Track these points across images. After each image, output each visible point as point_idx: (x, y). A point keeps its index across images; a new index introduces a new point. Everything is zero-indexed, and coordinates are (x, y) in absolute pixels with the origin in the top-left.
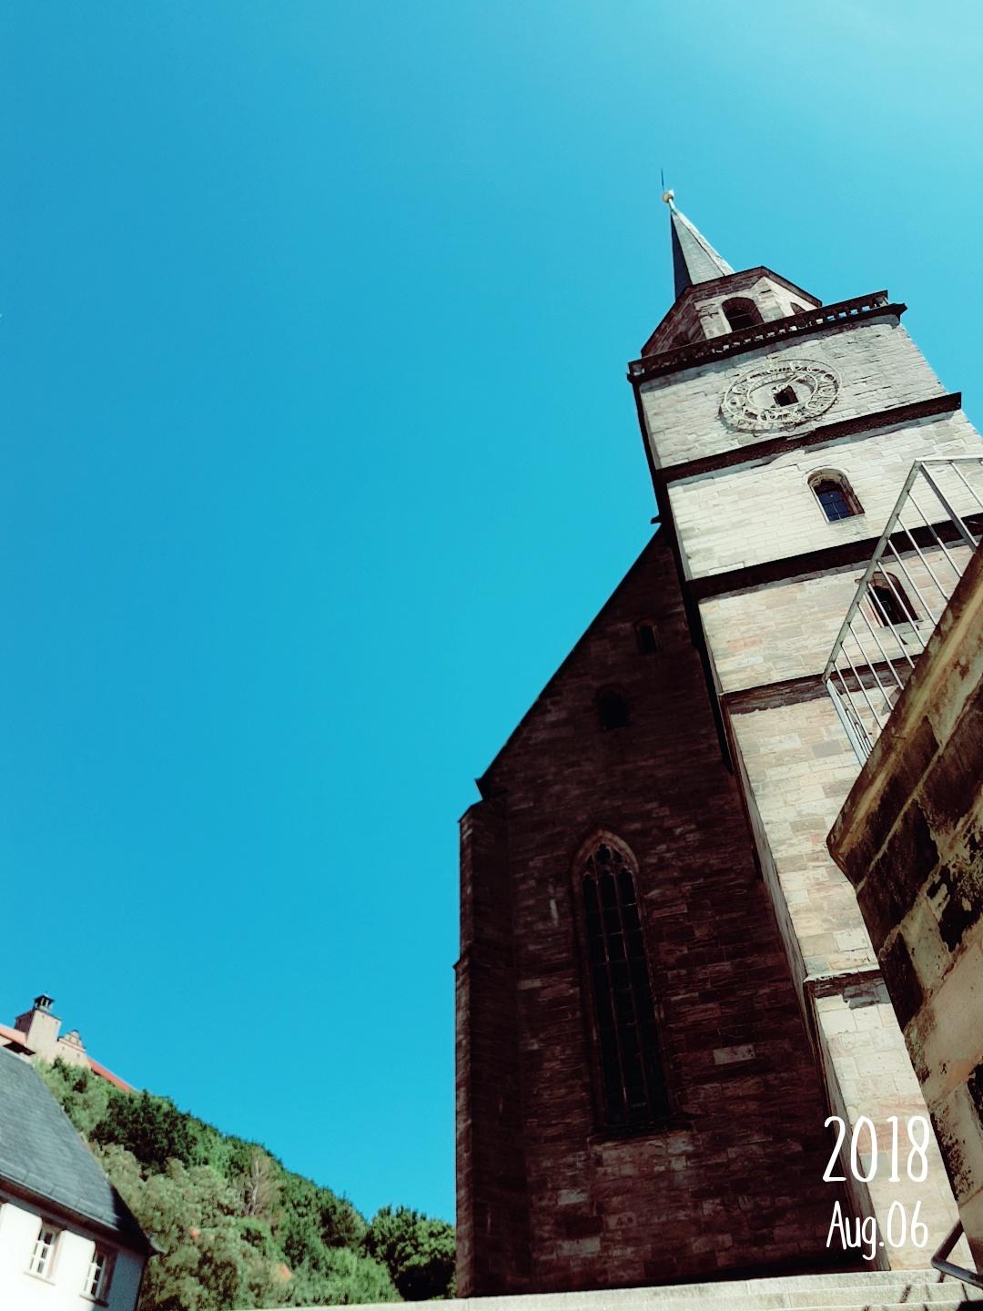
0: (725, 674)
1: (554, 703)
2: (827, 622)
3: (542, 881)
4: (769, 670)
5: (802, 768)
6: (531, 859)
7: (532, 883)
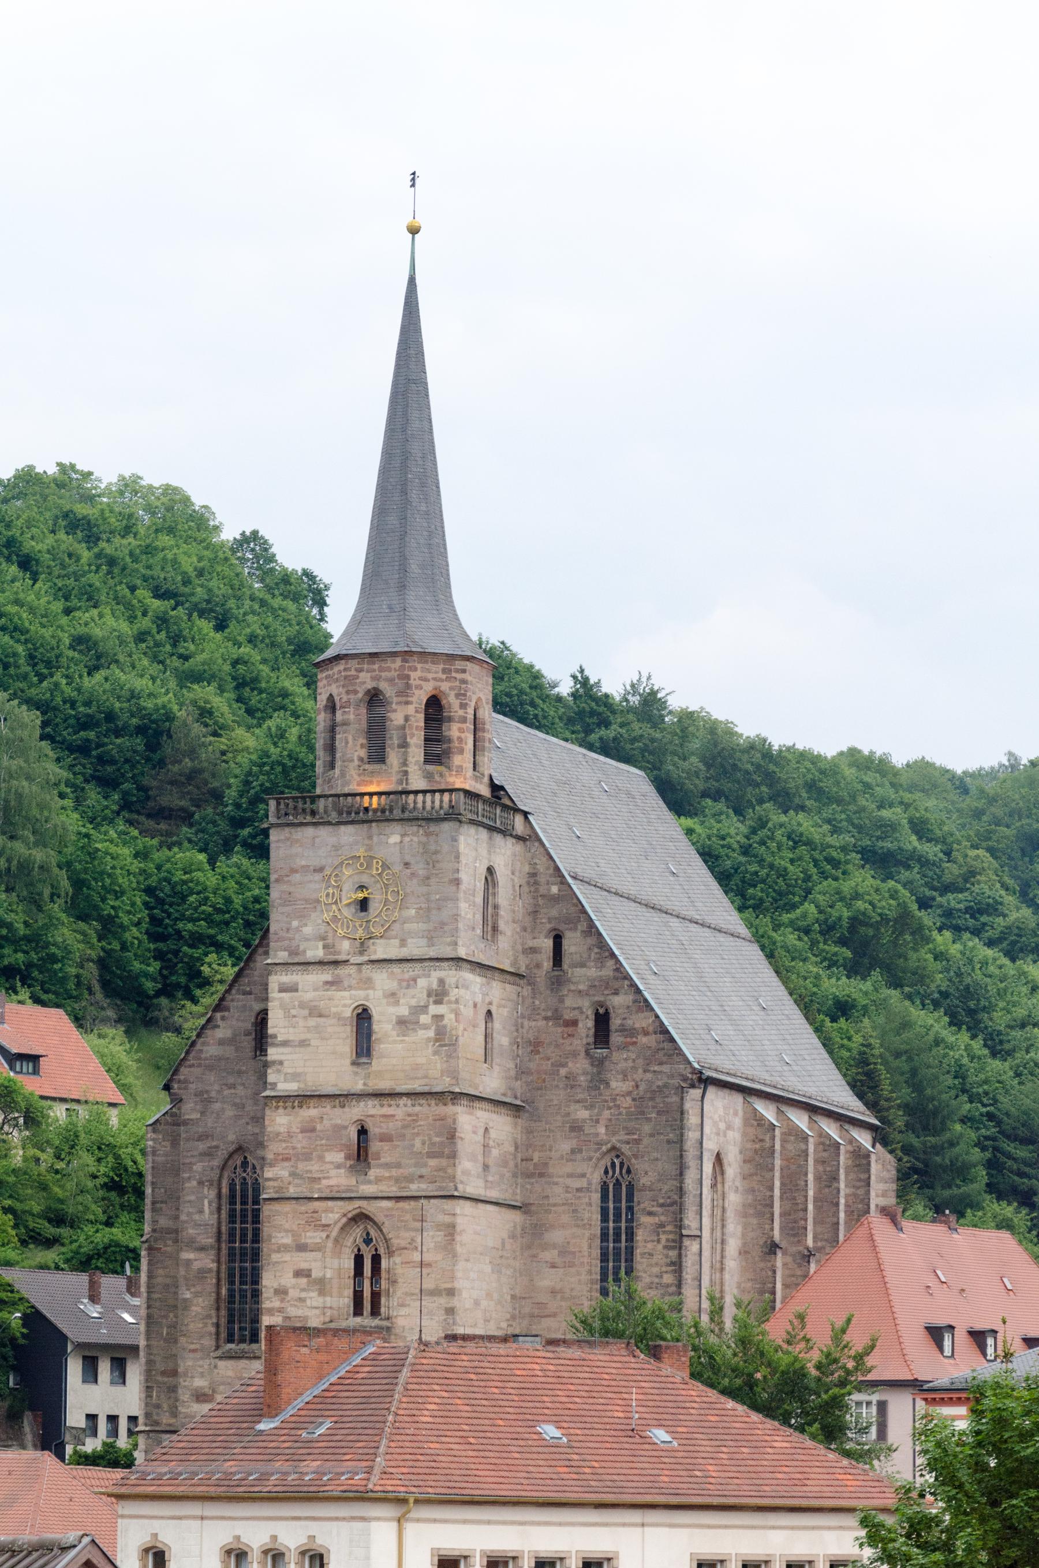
1: (223, 1018)
2: (327, 1154)
3: (201, 1183)
5: (287, 1257)
7: (194, 1183)
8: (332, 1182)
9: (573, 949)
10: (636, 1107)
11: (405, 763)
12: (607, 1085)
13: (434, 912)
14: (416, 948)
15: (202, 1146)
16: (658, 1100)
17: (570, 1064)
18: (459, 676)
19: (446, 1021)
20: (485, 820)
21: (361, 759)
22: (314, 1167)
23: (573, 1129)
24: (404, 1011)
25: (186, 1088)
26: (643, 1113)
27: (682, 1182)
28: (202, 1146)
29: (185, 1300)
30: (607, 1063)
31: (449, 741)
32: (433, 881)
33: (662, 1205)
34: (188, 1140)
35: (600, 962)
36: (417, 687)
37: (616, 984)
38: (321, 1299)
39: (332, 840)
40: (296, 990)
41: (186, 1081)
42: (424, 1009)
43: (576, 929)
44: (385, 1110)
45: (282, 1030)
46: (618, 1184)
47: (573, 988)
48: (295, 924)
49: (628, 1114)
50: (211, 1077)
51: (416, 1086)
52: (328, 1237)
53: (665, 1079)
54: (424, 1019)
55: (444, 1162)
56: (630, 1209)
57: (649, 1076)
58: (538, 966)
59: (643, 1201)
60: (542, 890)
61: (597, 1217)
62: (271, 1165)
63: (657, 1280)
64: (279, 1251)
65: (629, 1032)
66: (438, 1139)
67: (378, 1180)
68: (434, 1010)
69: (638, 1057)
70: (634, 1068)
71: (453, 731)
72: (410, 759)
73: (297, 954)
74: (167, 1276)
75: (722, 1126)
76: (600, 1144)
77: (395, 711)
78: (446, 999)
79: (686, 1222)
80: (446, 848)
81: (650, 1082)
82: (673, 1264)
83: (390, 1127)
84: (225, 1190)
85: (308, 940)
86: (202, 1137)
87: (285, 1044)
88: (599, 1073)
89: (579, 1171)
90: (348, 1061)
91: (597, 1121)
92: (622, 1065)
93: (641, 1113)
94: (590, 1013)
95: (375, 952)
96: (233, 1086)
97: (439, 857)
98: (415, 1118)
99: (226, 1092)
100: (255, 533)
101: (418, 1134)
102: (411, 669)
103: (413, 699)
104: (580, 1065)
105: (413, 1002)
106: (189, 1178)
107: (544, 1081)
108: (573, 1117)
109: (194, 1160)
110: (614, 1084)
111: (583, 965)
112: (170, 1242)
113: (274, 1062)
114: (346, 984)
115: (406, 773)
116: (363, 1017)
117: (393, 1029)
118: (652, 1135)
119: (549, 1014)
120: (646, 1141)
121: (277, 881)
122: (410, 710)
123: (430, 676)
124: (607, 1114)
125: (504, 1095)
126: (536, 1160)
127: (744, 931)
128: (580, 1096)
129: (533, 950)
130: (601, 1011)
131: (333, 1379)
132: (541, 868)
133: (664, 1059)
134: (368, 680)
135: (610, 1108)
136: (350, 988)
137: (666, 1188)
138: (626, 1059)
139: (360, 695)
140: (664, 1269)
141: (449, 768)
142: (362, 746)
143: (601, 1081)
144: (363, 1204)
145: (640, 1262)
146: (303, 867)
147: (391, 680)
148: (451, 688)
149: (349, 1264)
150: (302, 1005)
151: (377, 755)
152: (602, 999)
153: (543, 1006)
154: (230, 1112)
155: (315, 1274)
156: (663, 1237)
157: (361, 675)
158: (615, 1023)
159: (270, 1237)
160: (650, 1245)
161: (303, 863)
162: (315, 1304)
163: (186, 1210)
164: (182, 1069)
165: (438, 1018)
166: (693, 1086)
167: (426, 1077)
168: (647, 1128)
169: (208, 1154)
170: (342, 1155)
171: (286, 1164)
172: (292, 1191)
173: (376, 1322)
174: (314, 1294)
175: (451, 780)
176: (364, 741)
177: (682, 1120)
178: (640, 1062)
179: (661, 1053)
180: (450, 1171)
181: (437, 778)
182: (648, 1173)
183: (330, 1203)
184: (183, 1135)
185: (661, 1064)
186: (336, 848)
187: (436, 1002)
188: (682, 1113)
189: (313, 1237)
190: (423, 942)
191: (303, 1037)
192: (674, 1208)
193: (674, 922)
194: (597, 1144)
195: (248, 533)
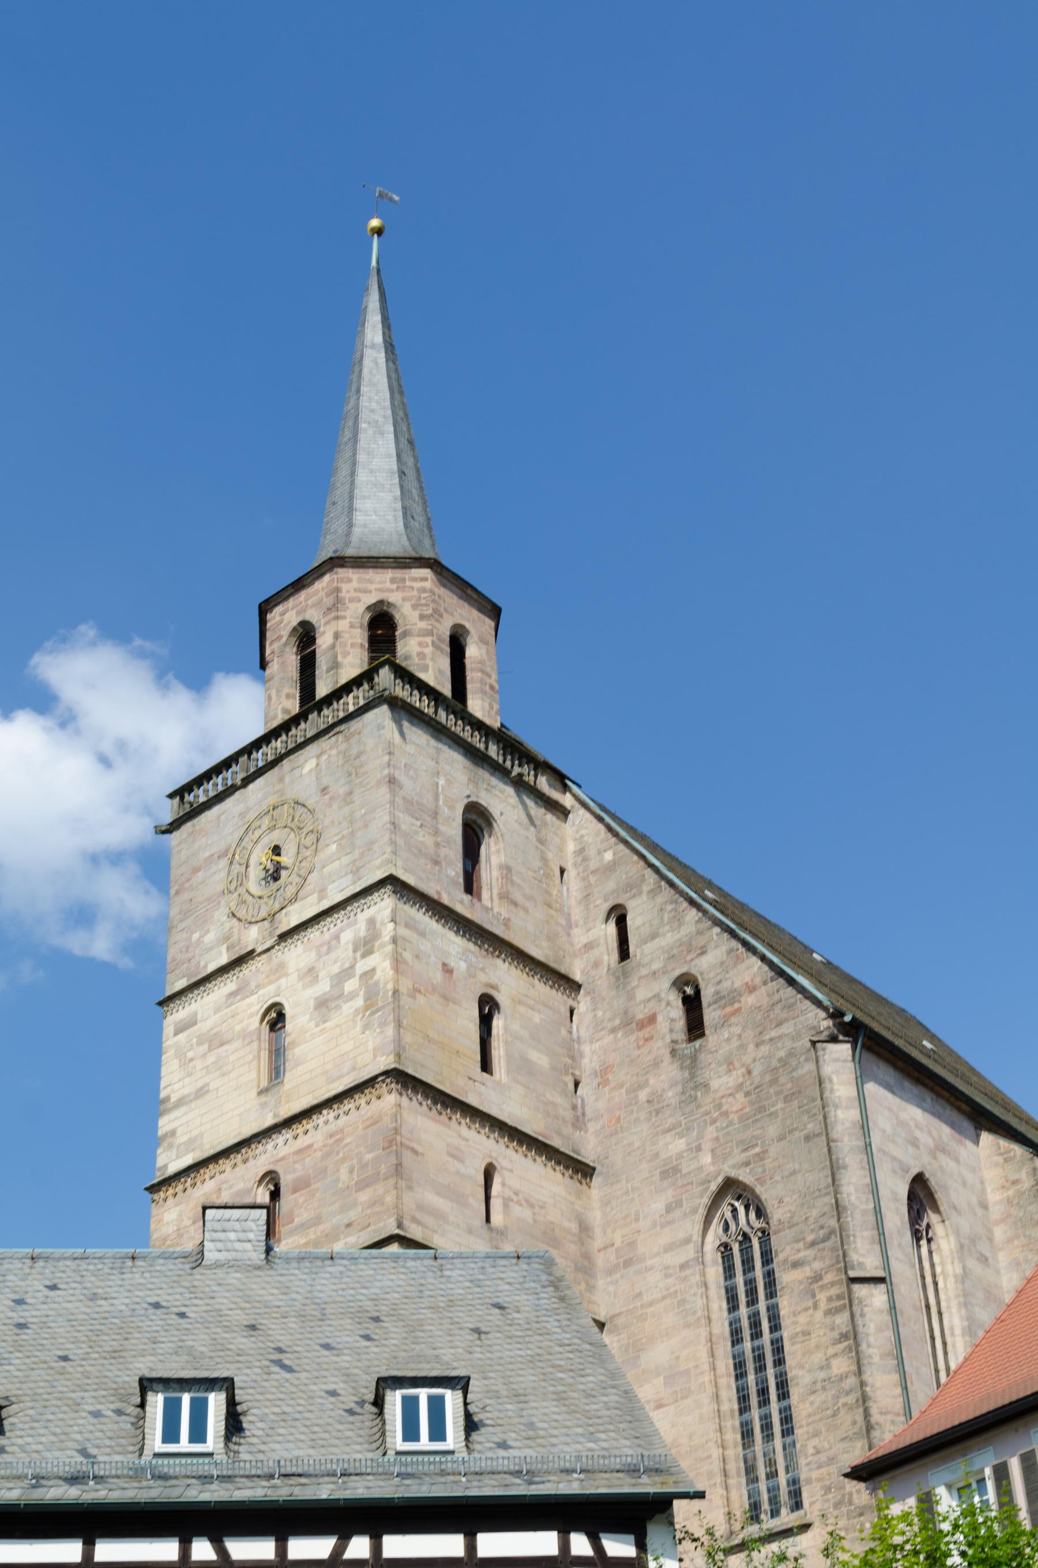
12: (706, 1086)
16: (782, 1080)
17: (652, 1081)
18: (417, 585)
19: (379, 974)
23: (665, 1175)
24: (324, 987)
26: (762, 1109)
35: (678, 920)
36: (351, 600)
37: (701, 941)
39: (241, 808)
40: (195, 1023)
47: (644, 972)
48: (196, 936)
49: (741, 1120)
53: (788, 1044)
54: (351, 985)
57: (764, 1049)
60: (593, 865)
63: (822, 1375)
65: (731, 998)
69: (744, 1029)
70: (742, 1047)
78: (377, 944)
79: (854, 1257)
80: (370, 743)
81: (768, 1057)
82: (844, 1336)
85: (211, 949)
87: (180, 1103)
88: (693, 1076)
89: (681, 1235)
90: (255, 1091)
91: (699, 1149)
93: (760, 1110)
97: (363, 758)
98: (337, 1137)
101: (344, 1160)
102: (342, 580)
103: (348, 613)
105: (336, 969)
107: (619, 1120)
108: (663, 1156)
110: (715, 1084)
111: (654, 936)
114: (253, 985)
116: (276, 1018)
117: (310, 1020)
118: (781, 1138)
120: (773, 1151)
122: (343, 625)
123: (372, 587)
124: (711, 1132)
126: (618, 1243)
128: (670, 1121)
129: (589, 946)
130: (689, 990)
133: (784, 1015)
135: (714, 1122)
137: (815, 1213)
138: (728, 1040)
139: (284, 639)
140: (831, 1351)
143: (696, 1088)
146: (206, 860)
148: (404, 599)
152: (684, 969)
153: (608, 1015)
156: (822, 1297)
157: (286, 617)
160: (802, 1319)
161: (207, 854)
166: (833, 1039)
178: (750, 1033)
179: (778, 1009)
185: (779, 1024)
186: (242, 815)
191: (200, 1084)
192: (835, 1240)
194: (703, 1183)
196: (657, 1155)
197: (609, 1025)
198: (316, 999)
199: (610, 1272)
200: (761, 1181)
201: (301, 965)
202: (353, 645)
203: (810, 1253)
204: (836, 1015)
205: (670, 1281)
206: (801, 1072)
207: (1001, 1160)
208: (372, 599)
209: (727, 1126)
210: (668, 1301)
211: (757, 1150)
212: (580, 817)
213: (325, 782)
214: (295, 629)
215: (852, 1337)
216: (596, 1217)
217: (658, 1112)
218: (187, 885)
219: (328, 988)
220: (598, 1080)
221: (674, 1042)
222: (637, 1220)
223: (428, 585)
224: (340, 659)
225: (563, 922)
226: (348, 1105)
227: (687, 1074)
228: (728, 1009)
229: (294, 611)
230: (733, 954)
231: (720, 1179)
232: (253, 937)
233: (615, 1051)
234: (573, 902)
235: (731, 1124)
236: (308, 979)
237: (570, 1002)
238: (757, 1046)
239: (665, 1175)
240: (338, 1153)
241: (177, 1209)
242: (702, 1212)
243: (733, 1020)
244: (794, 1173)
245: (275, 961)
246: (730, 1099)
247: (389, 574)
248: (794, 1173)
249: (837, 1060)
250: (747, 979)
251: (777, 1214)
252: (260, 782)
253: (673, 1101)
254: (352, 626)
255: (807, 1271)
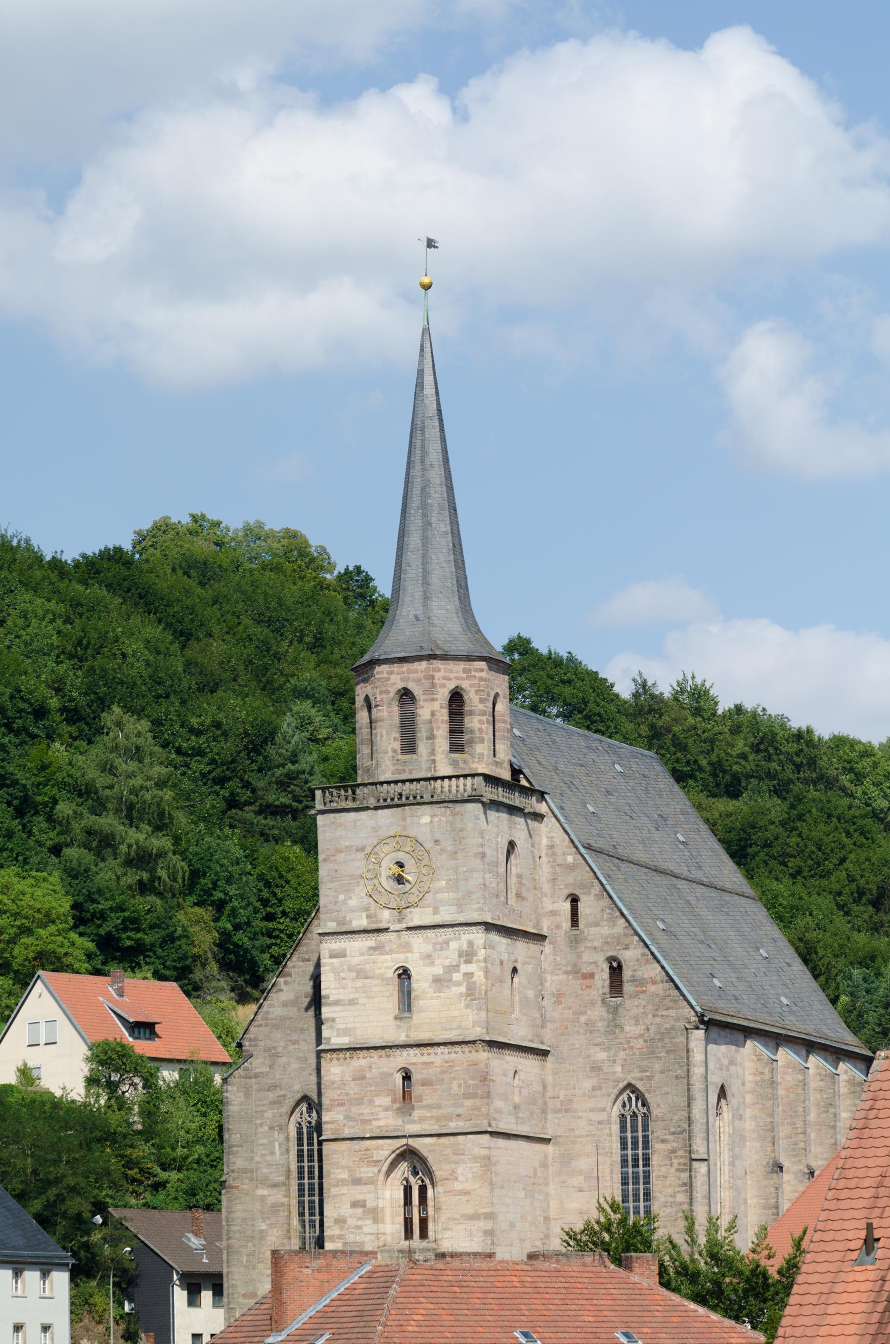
0: (327, 1123)
1: (286, 983)
2: (376, 1099)
3: (271, 1128)
4: (344, 1126)
5: (344, 1190)
6: (266, 1111)
7: (266, 1128)
8: (382, 1123)
9: (588, 911)
10: (647, 1047)
11: (433, 753)
13: (462, 883)
14: (447, 915)
15: (271, 1096)
16: (666, 1041)
17: (589, 1013)
18: (478, 674)
20: (505, 800)
21: (394, 751)
22: (365, 1110)
23: (593, 1069)
24: (439, 970)
25: (256, 1046)
26: (653, 1053)
27: (689, 1113)
28: (271, 1096)
29: (262, 1231)
30: (621, 1010)
31: (472, 732)
32: (460, 855)
33: (673, 1133)
34: (259, 1090)
35: (612, 922)
37: (627, 941)
38: (375, 1226)
40: (345, 956)
41: (255, 1039)
42: (456, 968)
43: (590, 893)
44: (426, 1058)
45: (334, 992)
46: (634, 1115)
47: (588, 944)
48: (341, 897)
49: (640, 1054)
50: (278, 1035)
51: (452, 1036)
52: (379, 1171)
53: (672, 1022)
54: (457, 977)
55: (478, 1102)
56: (646, 1139)
57: (658, 1020)
58: (558, 927)
59: (657, 1130)
60: (559, 860)
61: (617, 1145)
62: (328, 1110)
63: (671, 1199)
64: (337, 1185)
66: (471, 1082)
67: (422, 1120)
68: (464, 968)
70: (645, 1014)
71: (475, 723)
72: (437, 749)
73: (344, 924)
74: (245, 1211)
75: (725, 1062)
76: (618, 1081)
77: (422, 707)
78: (475, 958)
79: (695, 1147)
80: (470, 826)
82: (685, 1184)
83: (431, 1073)
84: (293, 1133)
85: (354, 911)
86: (272, 1087)
87: (337, 1003)
88: (614, 1019)
89: (600, 1105)
90: (392, 1017)
91: (614, 1061)
92: (635, 1011)
94: (606, 967)
95: (412, 920)
96: (296, 1042)
98: (450, 1065)
99: (291, 1048)
100: (358, 569)
101: (455, 1079)
102: (434, 670)
103: (438, 696)
104: (598, 1013)
105: (447, 962)
106: (261, 1124)
107: (567, 1028)
109: (265, 1108)
110: (627, 1028)
111: (597, 925)
112: (247, 1181)
113: (328, 1019)
114: (387, 949)
115: (434, 761)
116: (404, 974)
117: (430, 987)
118: (662, 1072)
119: (569, 968)
120: (657, 1077)
121: (324, 860)
122: (436, 706)
124: (622, 1055)
125: (531, 1041)
126: (562, 1098)
127: (747, 889)
128: (599, 1040)
129: (554, 913)
130: (615, 964)
131: (334, 1295)
132: (557, 841)
133: (671, 1004)
134: (398, 681)
135: (624, 1050)
136: (392, 952)
137: (676, 1117)
138: (637, 1006)
139: (392, 695)
140: (677, 1189)
141: (472, 756)
142: (395, 739)
143: (616, 1026)
144: (411, 1142)
145: (656, 1185)
146: (347, 847)
147: (418, 681)
148: (471, 686)
149: (401, 1194)
150: (350, 969)
151: (409, 746)
153: (564, 962)
154: (295, 1065)
155: (369, 1204)
157: (393, 677)
158: (627, 974)
159: (329, 1172)
160: (664, 1169)
161: (347, 844)
162: (370, 1231)
163: (259, 1152)
164: (252, 1029)
165: (469, 975)
166: (697, 1028)
167: (460, 1028)
168: (657, 1066)
169: (278, 1102)
170: (389, 1099)
171: (341, 1108)
172: (347, 1133)
173: (424, 1244)
174: (369, 1222)
175: (474, 766)
176: (398, 735)
177: (688, 1058)
178: (650, 1008)
179: (668, 1000)
180: (483, 1109)
181: (461, 764)
182: (662, 1104)
183: (380, 1141)
184: (255, 1087)
186: (375, 830)
187: (466, 962)
188: (688, 1052)
189: (366, 1172)
190: (453, 909)
191: (351, 996)
193: (682, 885)
194: (615, 1081)
195: (351, 569)
196: (589, 1056)
197: (564, 968)
198: (433, 976)
199: (557, 1111)
200: (649, 1092)
201: (422, 951)
202: (442, 721)
203: (671, 1137)
204: (701, 1018)
205: (592, 1128)
206: (676, 1040)
207: (756, 1058)
208: (451, 685)
209: (633, 1055)
210: (589, 1138)
211: (648, 1074)
212: (550, 821)
213: (437, 837)
214: (399, 690)
215: (689, 1186)
216: (550, 1079)
217: (591, 1032)
218: (332, 858)
219: (441, 972)
220: (555, 999)
221: (604, 994)
222: (574, 1089)
223: (484, 675)
224: (435, 732)
225: (539, 896)
226: (457, 1048)
227: (611, 1016)
228: (639, 989)
229: (399, 676)
230: (645, 957)
231: (625, 1083)
232: (385, 917)
233: (567, 985)
234: (543, 879)
235: (634, 1054)
236: (427, 961)
237: (542, 948)
238: (654, 1016)
239: (593, 1069)
240: (451, 1073)
241: (341, 1068)
242: (613, 1096)
243: (641, 996)
244: (667, 1093)
245: (403, 940)
246: (635, 1041)
247: (462, 665)
248: (667, 1093)
249: (697, 1039)
250: (652, 975)
251: (656, 1112)
252: (386, 811)
253: (601, 1029)
254: (441, 707)
255: (669, 1146)
